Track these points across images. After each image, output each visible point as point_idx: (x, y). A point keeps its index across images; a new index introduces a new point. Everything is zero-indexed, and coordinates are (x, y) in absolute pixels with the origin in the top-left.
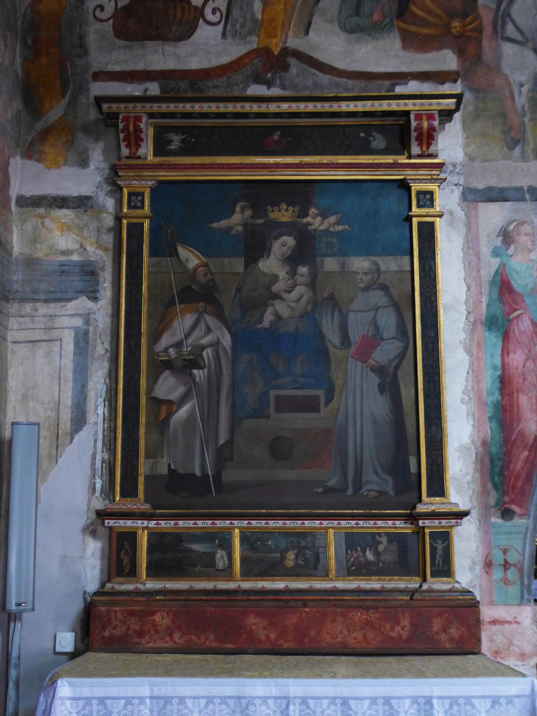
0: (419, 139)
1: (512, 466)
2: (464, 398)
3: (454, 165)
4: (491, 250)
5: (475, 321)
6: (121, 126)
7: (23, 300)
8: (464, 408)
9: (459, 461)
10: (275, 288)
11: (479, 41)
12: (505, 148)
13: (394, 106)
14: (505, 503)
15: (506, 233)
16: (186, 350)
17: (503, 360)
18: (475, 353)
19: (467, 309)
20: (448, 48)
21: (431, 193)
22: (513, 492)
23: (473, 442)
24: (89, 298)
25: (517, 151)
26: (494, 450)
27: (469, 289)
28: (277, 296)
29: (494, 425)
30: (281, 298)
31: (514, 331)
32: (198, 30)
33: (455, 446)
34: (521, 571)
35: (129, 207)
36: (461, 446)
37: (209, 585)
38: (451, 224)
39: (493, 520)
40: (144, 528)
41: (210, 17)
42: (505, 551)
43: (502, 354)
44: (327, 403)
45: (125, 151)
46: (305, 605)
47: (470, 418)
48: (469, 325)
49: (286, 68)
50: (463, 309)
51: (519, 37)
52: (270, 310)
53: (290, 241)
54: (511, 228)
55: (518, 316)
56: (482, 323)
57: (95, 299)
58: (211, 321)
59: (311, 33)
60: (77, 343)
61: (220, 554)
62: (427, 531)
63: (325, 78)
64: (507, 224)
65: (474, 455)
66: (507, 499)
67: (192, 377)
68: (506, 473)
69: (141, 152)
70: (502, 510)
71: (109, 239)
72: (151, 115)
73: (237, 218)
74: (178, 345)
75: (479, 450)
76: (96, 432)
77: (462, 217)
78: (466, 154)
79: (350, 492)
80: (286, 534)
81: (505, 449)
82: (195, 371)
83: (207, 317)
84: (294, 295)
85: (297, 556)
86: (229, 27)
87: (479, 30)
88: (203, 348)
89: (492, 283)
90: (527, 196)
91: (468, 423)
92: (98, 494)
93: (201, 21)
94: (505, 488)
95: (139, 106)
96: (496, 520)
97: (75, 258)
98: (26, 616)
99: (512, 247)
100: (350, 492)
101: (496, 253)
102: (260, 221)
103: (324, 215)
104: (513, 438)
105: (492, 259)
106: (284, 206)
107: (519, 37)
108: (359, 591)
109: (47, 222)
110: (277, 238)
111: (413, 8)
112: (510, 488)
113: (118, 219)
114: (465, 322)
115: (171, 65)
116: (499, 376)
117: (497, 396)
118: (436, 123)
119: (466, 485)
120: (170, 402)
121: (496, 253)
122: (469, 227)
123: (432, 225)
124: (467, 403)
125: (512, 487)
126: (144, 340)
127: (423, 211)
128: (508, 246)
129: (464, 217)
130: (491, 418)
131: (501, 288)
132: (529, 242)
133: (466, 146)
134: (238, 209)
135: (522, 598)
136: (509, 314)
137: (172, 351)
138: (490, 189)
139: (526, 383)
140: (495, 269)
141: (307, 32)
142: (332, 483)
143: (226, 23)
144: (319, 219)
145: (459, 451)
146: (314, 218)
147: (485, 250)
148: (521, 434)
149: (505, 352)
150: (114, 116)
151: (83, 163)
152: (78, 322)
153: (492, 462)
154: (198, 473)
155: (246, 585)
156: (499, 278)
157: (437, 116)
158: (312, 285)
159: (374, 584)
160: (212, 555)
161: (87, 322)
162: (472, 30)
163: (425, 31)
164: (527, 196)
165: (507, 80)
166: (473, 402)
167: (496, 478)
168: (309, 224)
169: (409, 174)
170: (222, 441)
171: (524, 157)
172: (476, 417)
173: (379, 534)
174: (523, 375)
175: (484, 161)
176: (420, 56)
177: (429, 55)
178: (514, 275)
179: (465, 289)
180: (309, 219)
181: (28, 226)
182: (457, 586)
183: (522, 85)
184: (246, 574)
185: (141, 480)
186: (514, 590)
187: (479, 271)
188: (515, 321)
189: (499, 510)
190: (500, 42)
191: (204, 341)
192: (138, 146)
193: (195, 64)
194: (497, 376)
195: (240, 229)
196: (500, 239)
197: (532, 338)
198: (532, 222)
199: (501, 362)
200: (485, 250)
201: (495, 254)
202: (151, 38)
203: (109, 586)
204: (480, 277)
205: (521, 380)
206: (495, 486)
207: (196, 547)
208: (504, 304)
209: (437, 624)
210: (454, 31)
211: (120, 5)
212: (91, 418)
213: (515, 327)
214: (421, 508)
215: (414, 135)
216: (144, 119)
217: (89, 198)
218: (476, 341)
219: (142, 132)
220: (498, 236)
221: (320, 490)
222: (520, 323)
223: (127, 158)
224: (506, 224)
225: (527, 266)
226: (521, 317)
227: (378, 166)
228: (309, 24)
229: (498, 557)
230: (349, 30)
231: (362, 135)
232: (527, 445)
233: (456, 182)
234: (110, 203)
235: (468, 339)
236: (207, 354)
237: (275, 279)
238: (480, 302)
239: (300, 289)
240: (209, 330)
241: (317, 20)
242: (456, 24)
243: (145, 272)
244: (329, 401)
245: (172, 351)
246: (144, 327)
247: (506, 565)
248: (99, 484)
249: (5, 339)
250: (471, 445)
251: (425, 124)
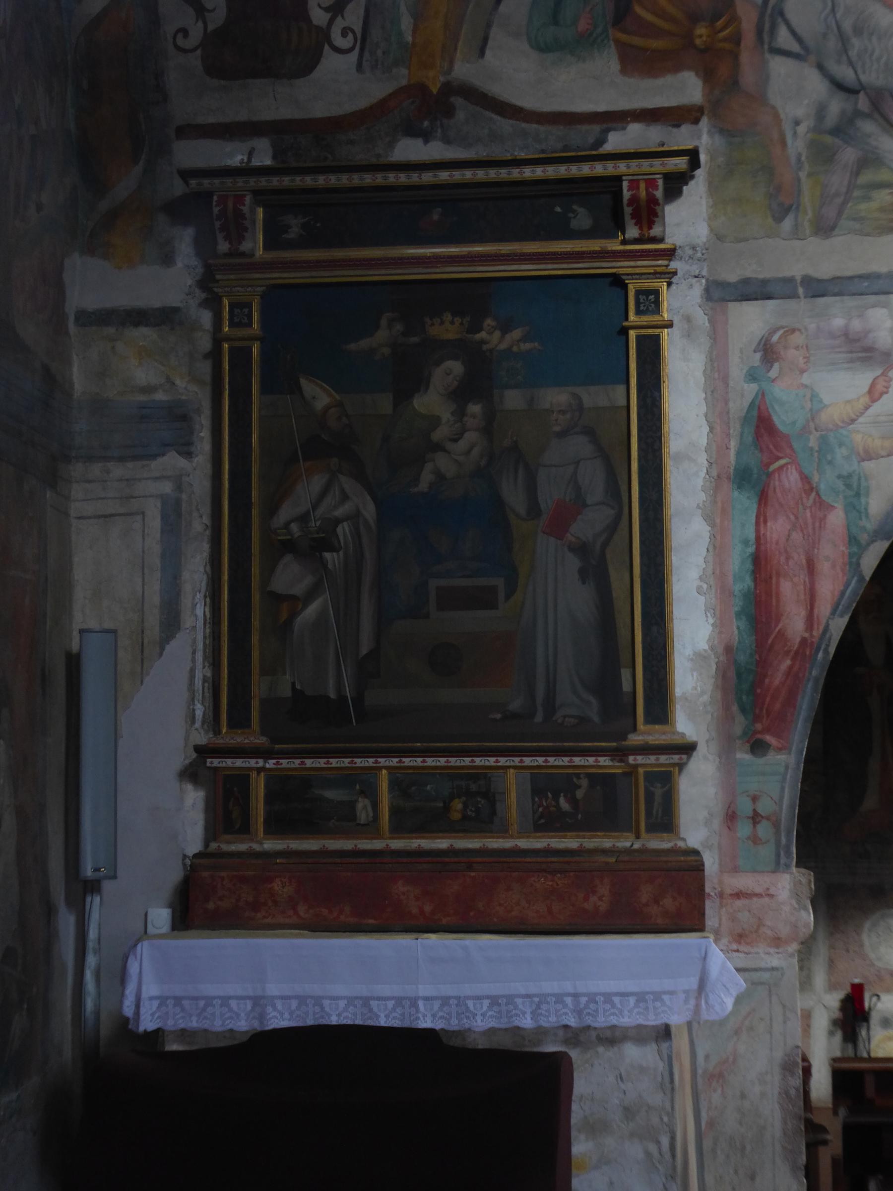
0: (637, 217)
1: (767, 681)
2: (701, 586)
3: (694, 248)
4: (745, 371)
5: (719, 476)
6: (216, 210)
8: (702, 599)
9: (693, 676)
10: (437, 435)
11: (736, 56)
12: (770, 220)
13: (599, 169)
14: (755, 732)
15: (768, 346)
16: (314, 524)
17: (757, 531)
18: (718, 521)
19: (708, 459)
20: (689, 68)
21: (656, 293)
22: (768, 716)
23: (712, 648)
24: (180, 454)
25: (787, 223)
26: (742, 658)
27: (712, 429)
28: (438, 447)
29: (743, 624)
30: (444, 450)
31: (775, 489)
32: (323, 60)
33: (687, 654)
34: (776, 825)
35: (232, 324)
36: (695, 654)
37: (347, 845)
38: (688, 335)
39: (739, 755)
40: (259, 770)
41: (339, 41)
42: (755, 799)
43: (757, 523)
44: (508, 597)
45: (223, 246)
46: (470, 867)
47: (709, 615)
48: (711, 482)
49: (449, 112)
50: (702, 459)
51: (795, 47)
52: (429, 466)
53: (456, 367)
54: (775, 338)
55: (781, 468)
56: (729, 478)
57: (189, 455)
58: (347, 483)
59: (488, 53)
60: (164, 517)
61: (363, 805)
62: (641, 771)
63: (506, 125)
64: (769, 334)
65: (714, 667)
66: (759, 726)
67: (324, 564)
68: (759, 691)
69: (246, 246)
70: (752, 742)
71: (205, 368)
72: (256, 193)
73: (382, 335)
74: (303, 519)
75: (721, 659)
76: (194, 641)
77: (704, 324)
78: (711, 230)
79: (539, 718)
80: (452, 774)
81: (757, 657)
82: (327, 555)
83: (340, 476)
84: (462, 445)
85: (465, 805)
86: (367, 55)
87: (736, 39)
88: (337, 521)
89: (745, 420)
90: (801, 291)
91: (707, 621)
92: (198, 724)
93: (326, 47)
94: (757, 711)
95: (240, 182)
96: (742, 756)
97: (160, 396)
98: (108, 886)
99: (776, 366)
100: (539, 718)
101: (752, 376)
102: (415, 339)
103: (505, 328)
104: (770, 641)
105: (746, 386)
106: (448, 317)
107: (795, 47)
108: (548, 852)
110: (438, 363)
111: (638, 10)
112: (764, 711)
113: (217, 342)
114: (705, 478)
115: (286, 113)
116: (751, 554)
117: (748, 582)
118: (659, 194)
119: (701, 708)
120: (293, 598)
121: (752, 376)
122: (715, 339)
123: (657, 339)
124: (705, 593)
125: (767, 710)
126: (255, 512)
127: (646, 319)
128: (769, 365)
129: (707, 324)
130: (738, 615)
131: (757, 427)
132: (801, 358)
133: (712, 218)
134: (384, 322)
135: (778, 863)
136: (768, 465)
137: (294, 527)
138: (746, 281)
139: (790, 563)
140: (750, 400)
141: (482, 53)
142: (516, 705)
143: (362, 49)
144: (497, 334)
145: (692, 660)
146: (490, 333)
147: (737, 370)
148: (781, 634)
149: (761, 519)
150: (204, 197)
151: (167, 259)
152: (167, 488)
153: (739, 675)
154: (332, 695)
155: (397, 844)
156: (755, 413)
157: (660, 183)
158: (488, 429)
159: (570, 842)
160: (352, 805)
161: (179, 488)
162: (725, 40)
163: (655, 44)
164: (801, 291)
165: (776, 116)
166: (713, 591)
167: (744, 697)
168: (483, 342)
169: (622, 267)
170: (364, 651)
171: (796, 234)
172: (718, 613)
173: (578, 776)
174: (786, 551)
175: (739, 240)
176: (648, 83)
177: (660, 81)
178: (777, 407)
179: (706, 429)
180: (483, 335)
182: (681, 844)
183: (797, 123)
184: (399, 828)
185: (255, 704)
186: (767, 852)
187: (726, 402)
188: (777, 475)
189: (748, 742)
190: (768, 55)
191: (339, 513)
192: (241, 239)
193: (320, 110)
194: (748, 554)
195: (386, 351)
196: (758, 355)
197: (801, 499)
198: (806, 329)
199: (754, 535)
200: (737, 370)
201: (751, 378)
203: (214, 846)
204: (728, 413)
205: (782, 559)
206: (743, 710)
207: (330, 794)
208: (761, 450)
209: (645, 894)
210: (698, 42)
211: (211, 28)
212: (187, 621)
213: (777, 483)
214: (634, 739)
215: (628, 210)
216: (248, 199)
217: (176, 310)
218: (719, 504)
219: (246, 219)
220: (755, 351)
221: (499, 716)
222: (783, 476)
223: (226, 255)
224: (767, 334)
225: (797, 395)
226: (785, 469)
227: (579, 256)
228: (485, 40)
229: (745, 806)
230: (542, 48)
231: (558, 209)
232: (789, 651)
233: (697, 273)
234: (206, 318)
235: (708, 502)
236: (344, 530)
237: (435, 421)
238: (727, 448)
239: (471, 436)
240: (345, 497)
241: (497, 35)
242: (701, 30)
243: (255, 416)
244: (510, 592)
245: (294, 527)
246: (254, 494)
247: (756, 818)
248: (199, 713)
249: (67, 514)
250: (709, 651)
251: (643, 193)
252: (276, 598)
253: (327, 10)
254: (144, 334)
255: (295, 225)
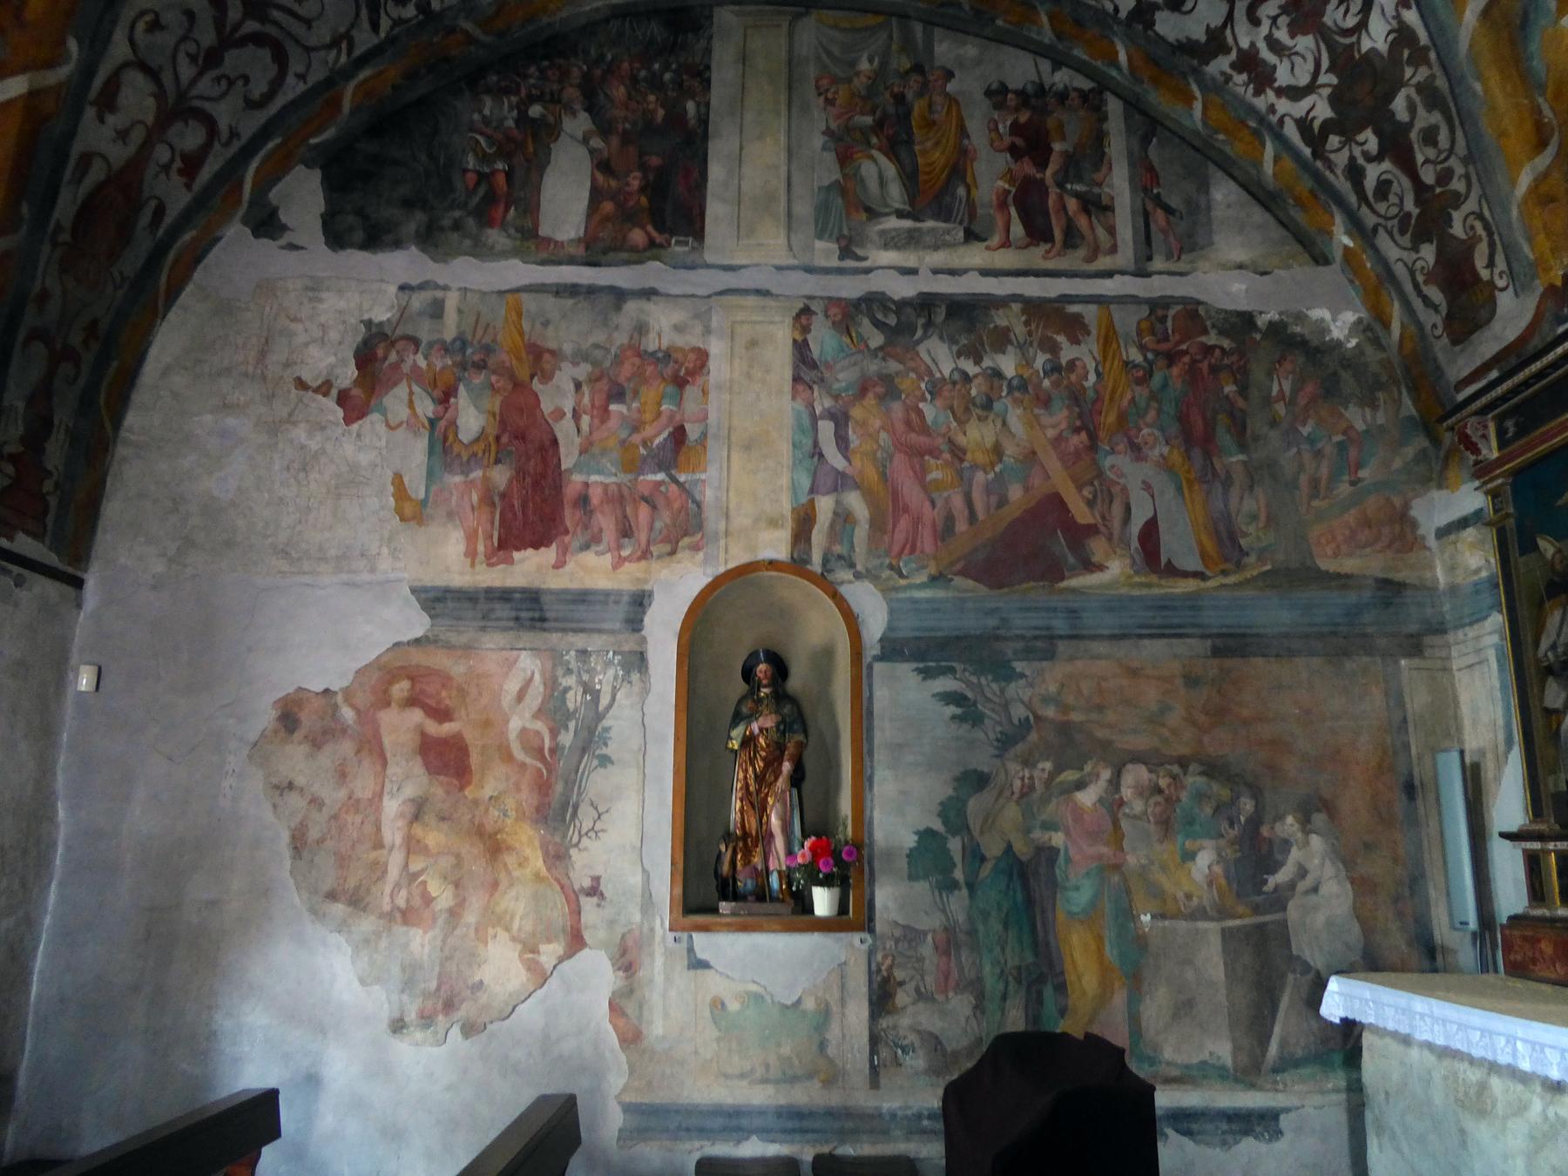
7: (1456, 628)
32: (1498, 302)
74: (1554, 647)
86: (1517, 285)
109: (1459, 545)
120: (1556, 711)
137: (1550, 654)
181: (1446, 556)
193: (1511, 335)
202: (1472, 332)
252: (1549, 712)
253: (1487, 267)
254: (1470, 534)
255: (1510, 424)
